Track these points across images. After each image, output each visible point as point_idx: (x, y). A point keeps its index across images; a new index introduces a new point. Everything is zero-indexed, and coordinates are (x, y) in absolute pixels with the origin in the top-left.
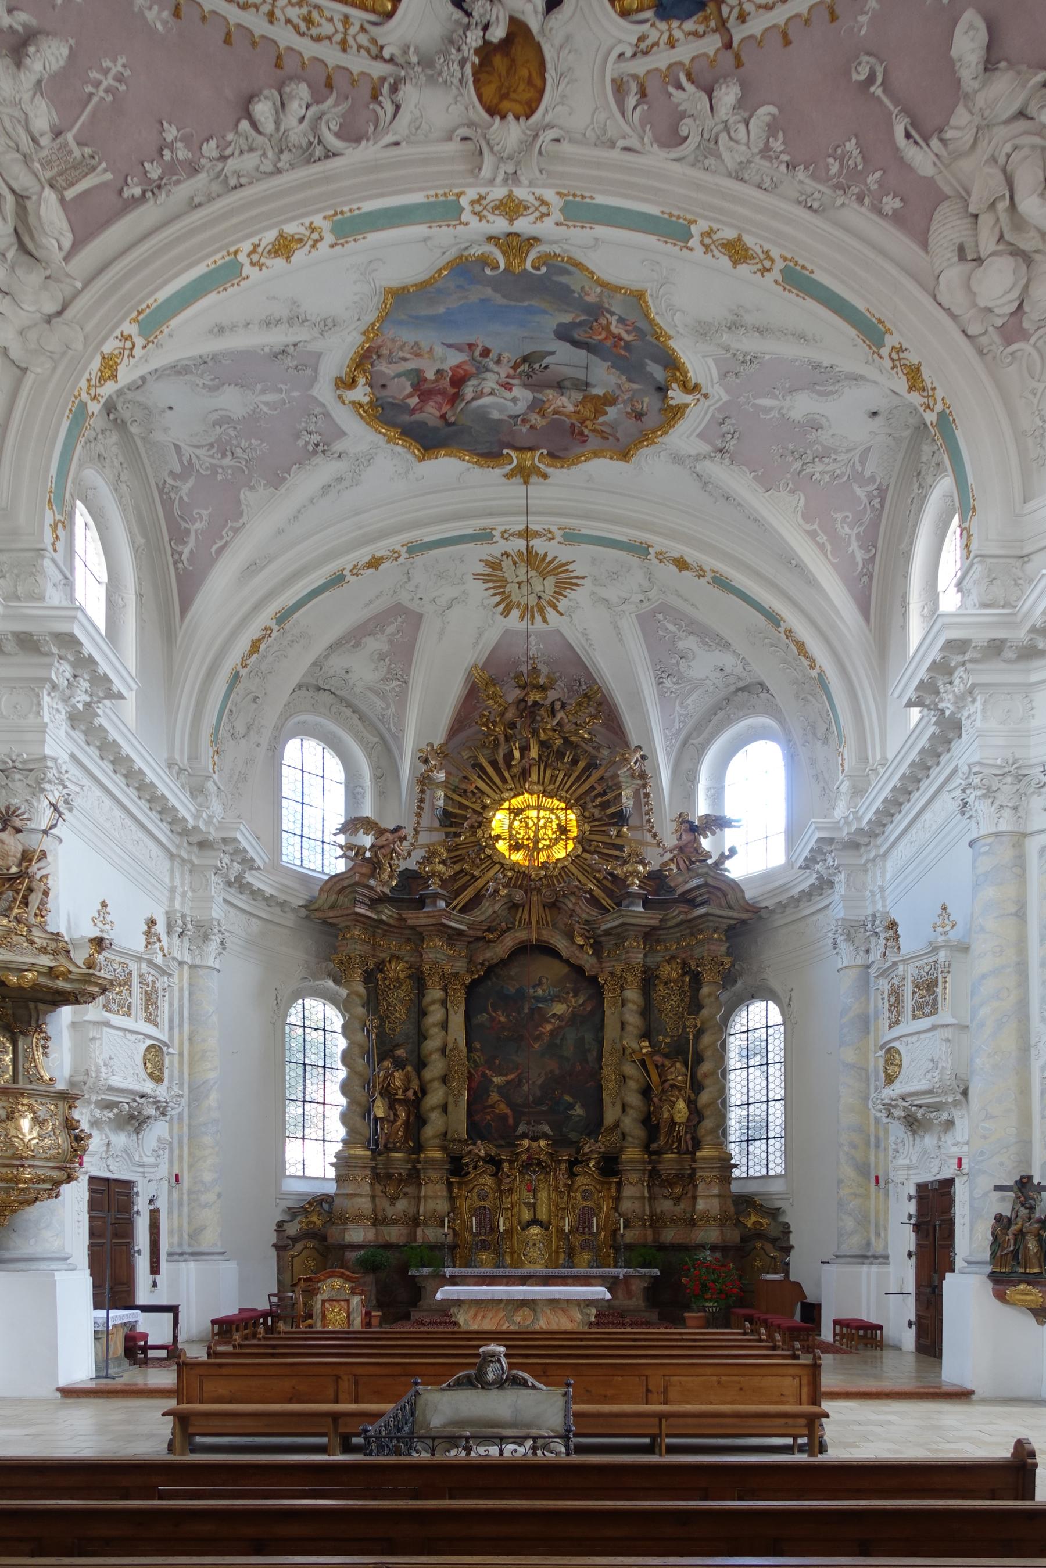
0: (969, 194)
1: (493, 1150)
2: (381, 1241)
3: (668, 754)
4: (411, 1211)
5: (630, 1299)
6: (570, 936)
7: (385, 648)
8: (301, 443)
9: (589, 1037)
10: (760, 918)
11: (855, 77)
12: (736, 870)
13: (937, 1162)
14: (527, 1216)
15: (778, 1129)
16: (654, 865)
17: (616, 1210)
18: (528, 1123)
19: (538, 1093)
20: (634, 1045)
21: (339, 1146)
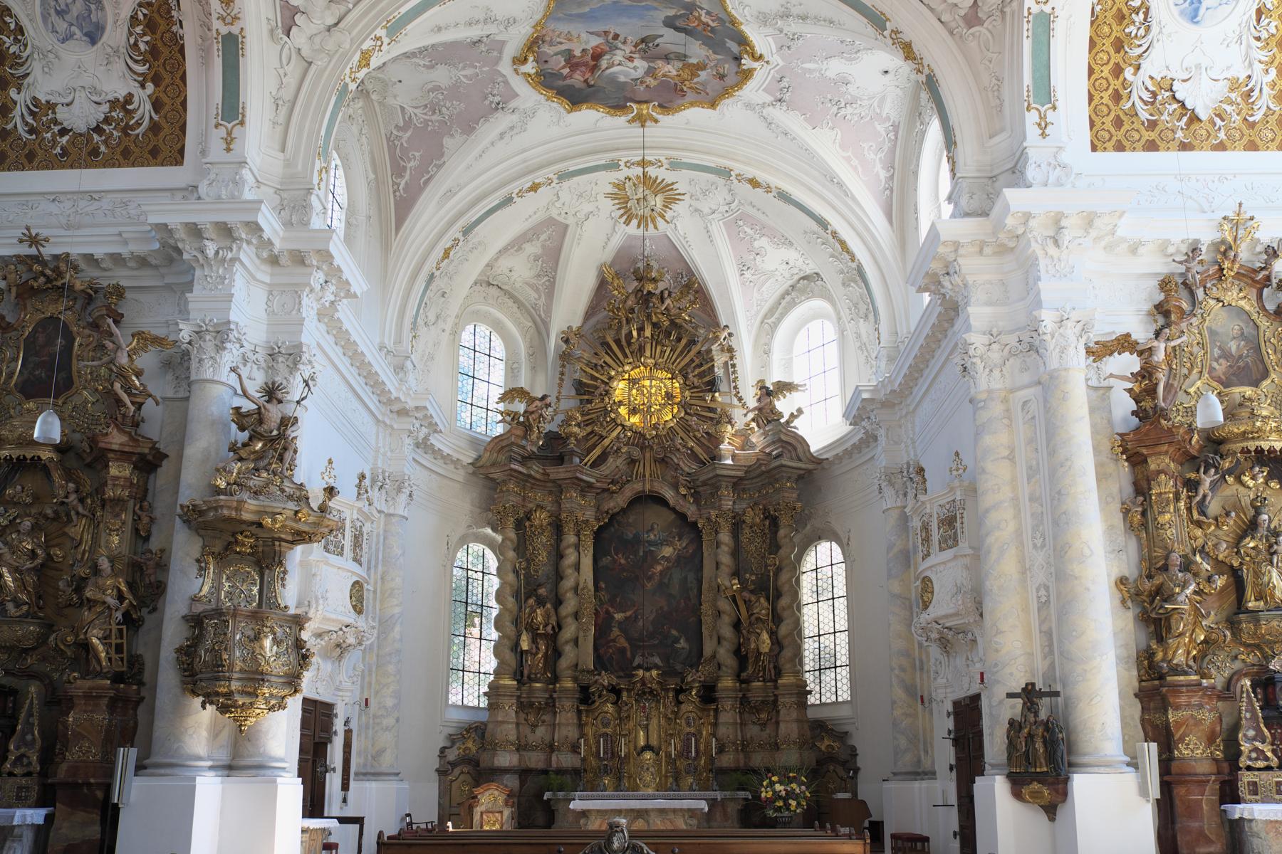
1: (615, 681)
2: (523, 766)
4: (547, 739)
6: (675, 487)
8: (487, 102)
9: (691, 577)
18: (643, 655)
19: (651, 628)
20: (727, 583)
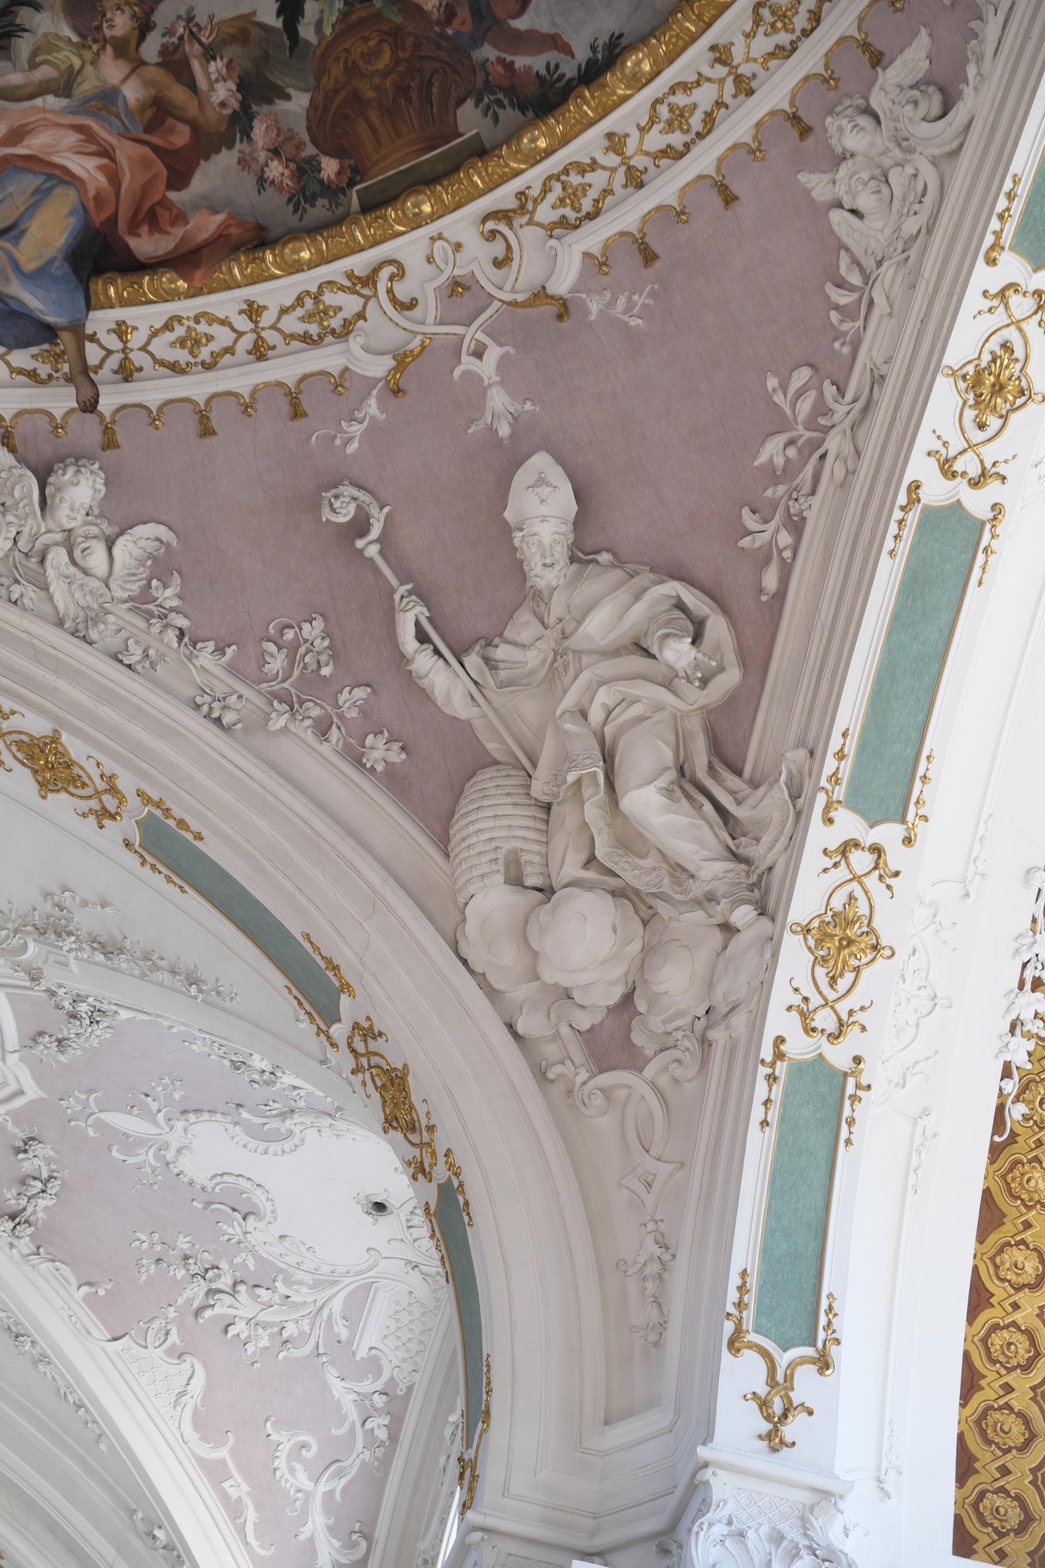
0: (535, 765)
11: (327, 515)
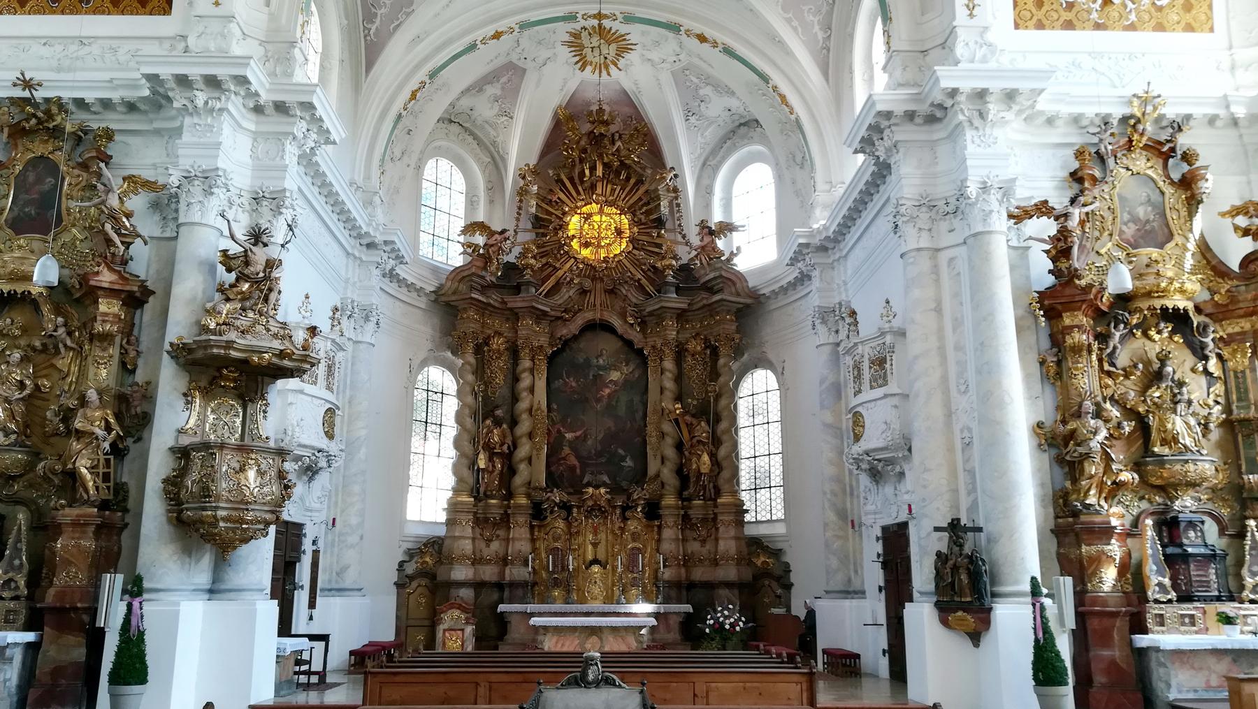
1: (566, 498)
2: (478, 579)
3: (693, 173)
5: (669, 632)
6: (623, 316)
7: (499, 92)
9: (637, 399)
10: (760, 302)
12: (742, 264)
13: (894, 508)
14: (590, 557)
15: (778, 479)
16: (684, 261)
17: (658, 550)
20: (671, 407)
21: (450, 494)
